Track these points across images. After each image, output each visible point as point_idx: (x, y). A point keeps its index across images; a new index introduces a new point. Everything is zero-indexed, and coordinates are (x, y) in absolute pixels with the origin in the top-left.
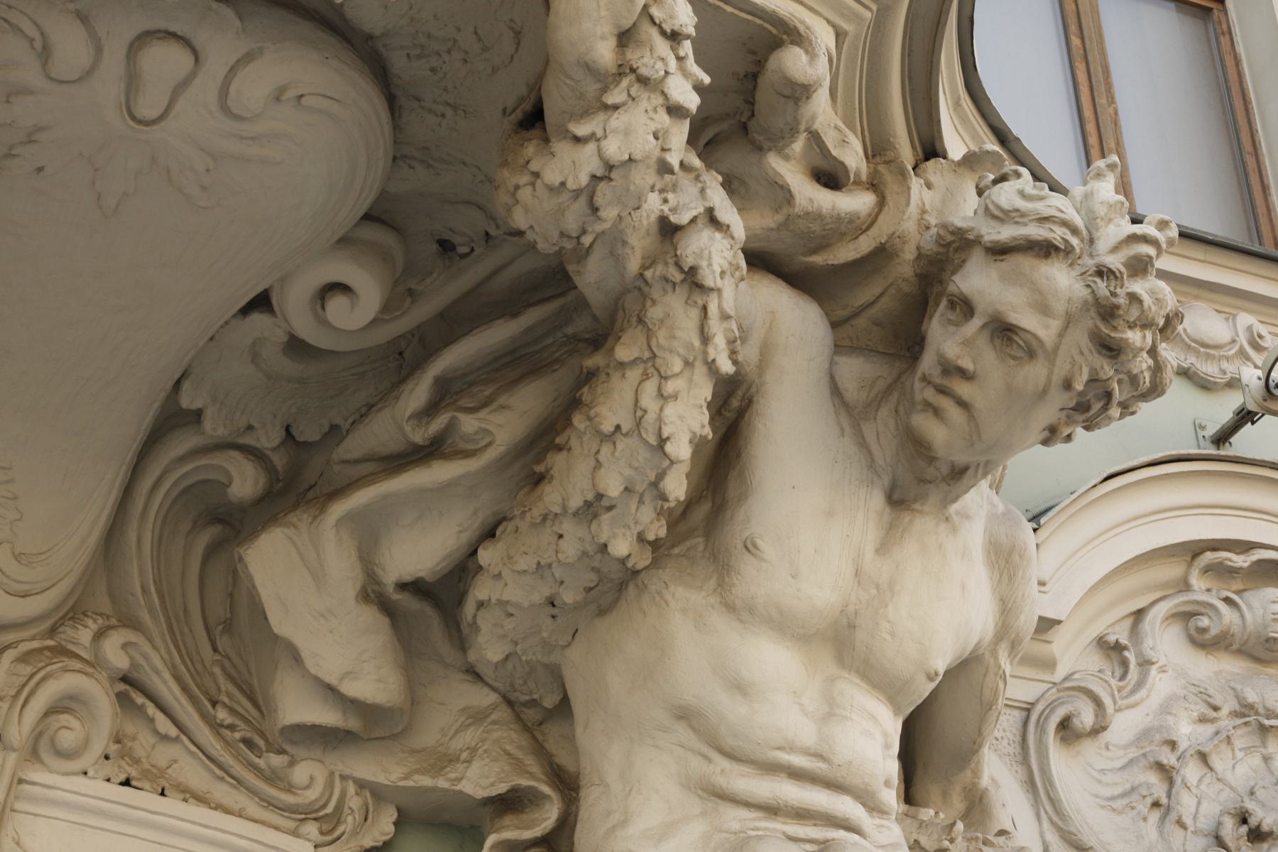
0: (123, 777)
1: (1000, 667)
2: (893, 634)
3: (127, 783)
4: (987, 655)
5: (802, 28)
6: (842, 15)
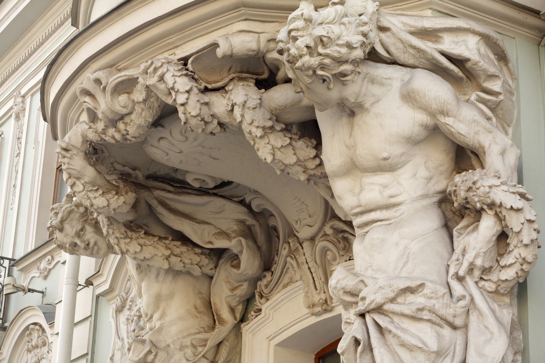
0: (348, 258)
1: (442, 123)
2: (362, 158)
3: (350, 260)
4: (437, 122)
5: (216, 42)
6: (239, 17)
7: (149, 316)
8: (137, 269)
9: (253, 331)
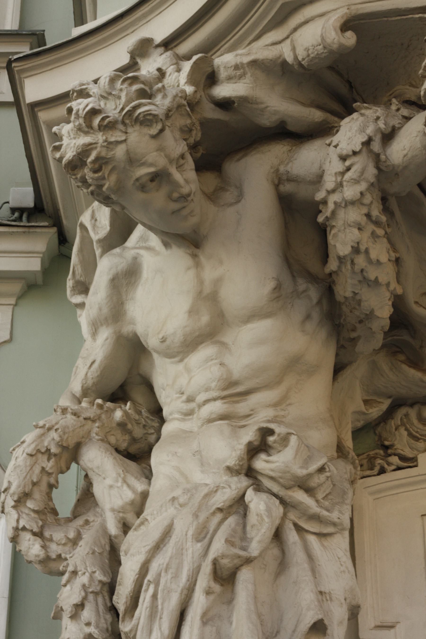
7: (240, 389)
8: (275, 289)
9: (380, 491)
